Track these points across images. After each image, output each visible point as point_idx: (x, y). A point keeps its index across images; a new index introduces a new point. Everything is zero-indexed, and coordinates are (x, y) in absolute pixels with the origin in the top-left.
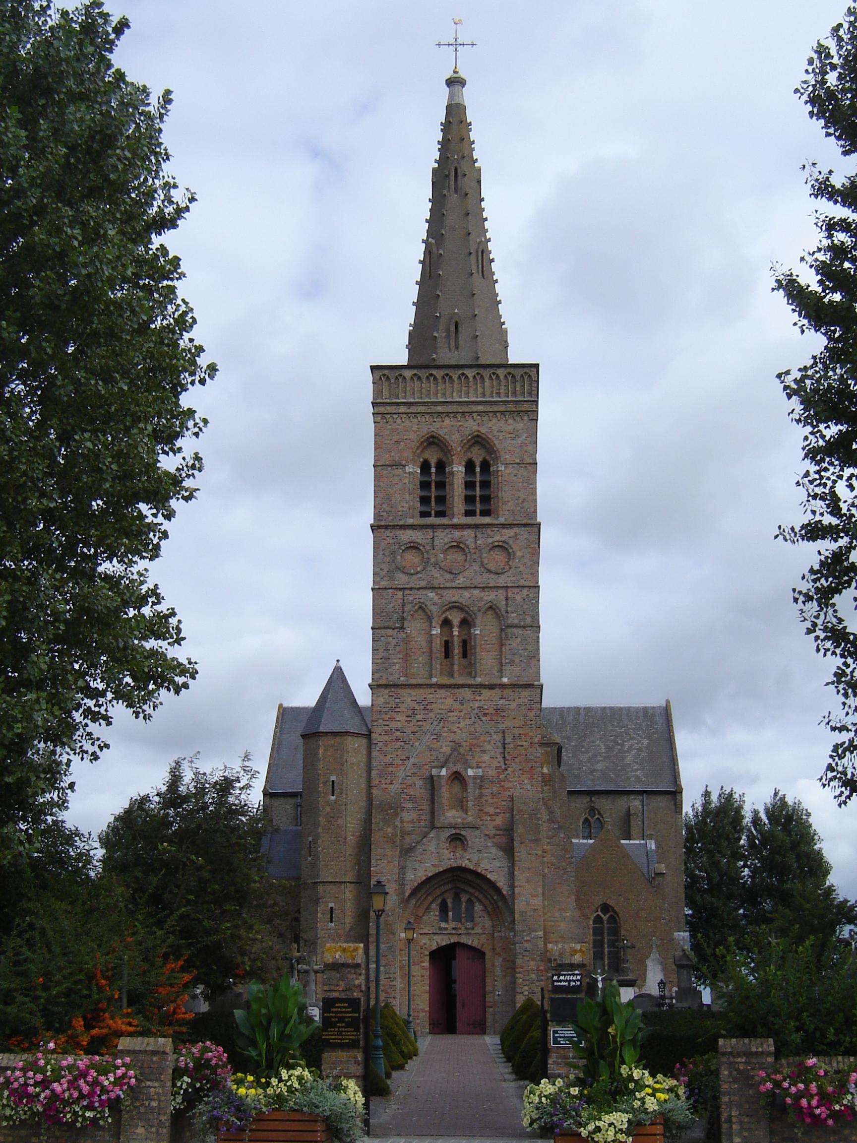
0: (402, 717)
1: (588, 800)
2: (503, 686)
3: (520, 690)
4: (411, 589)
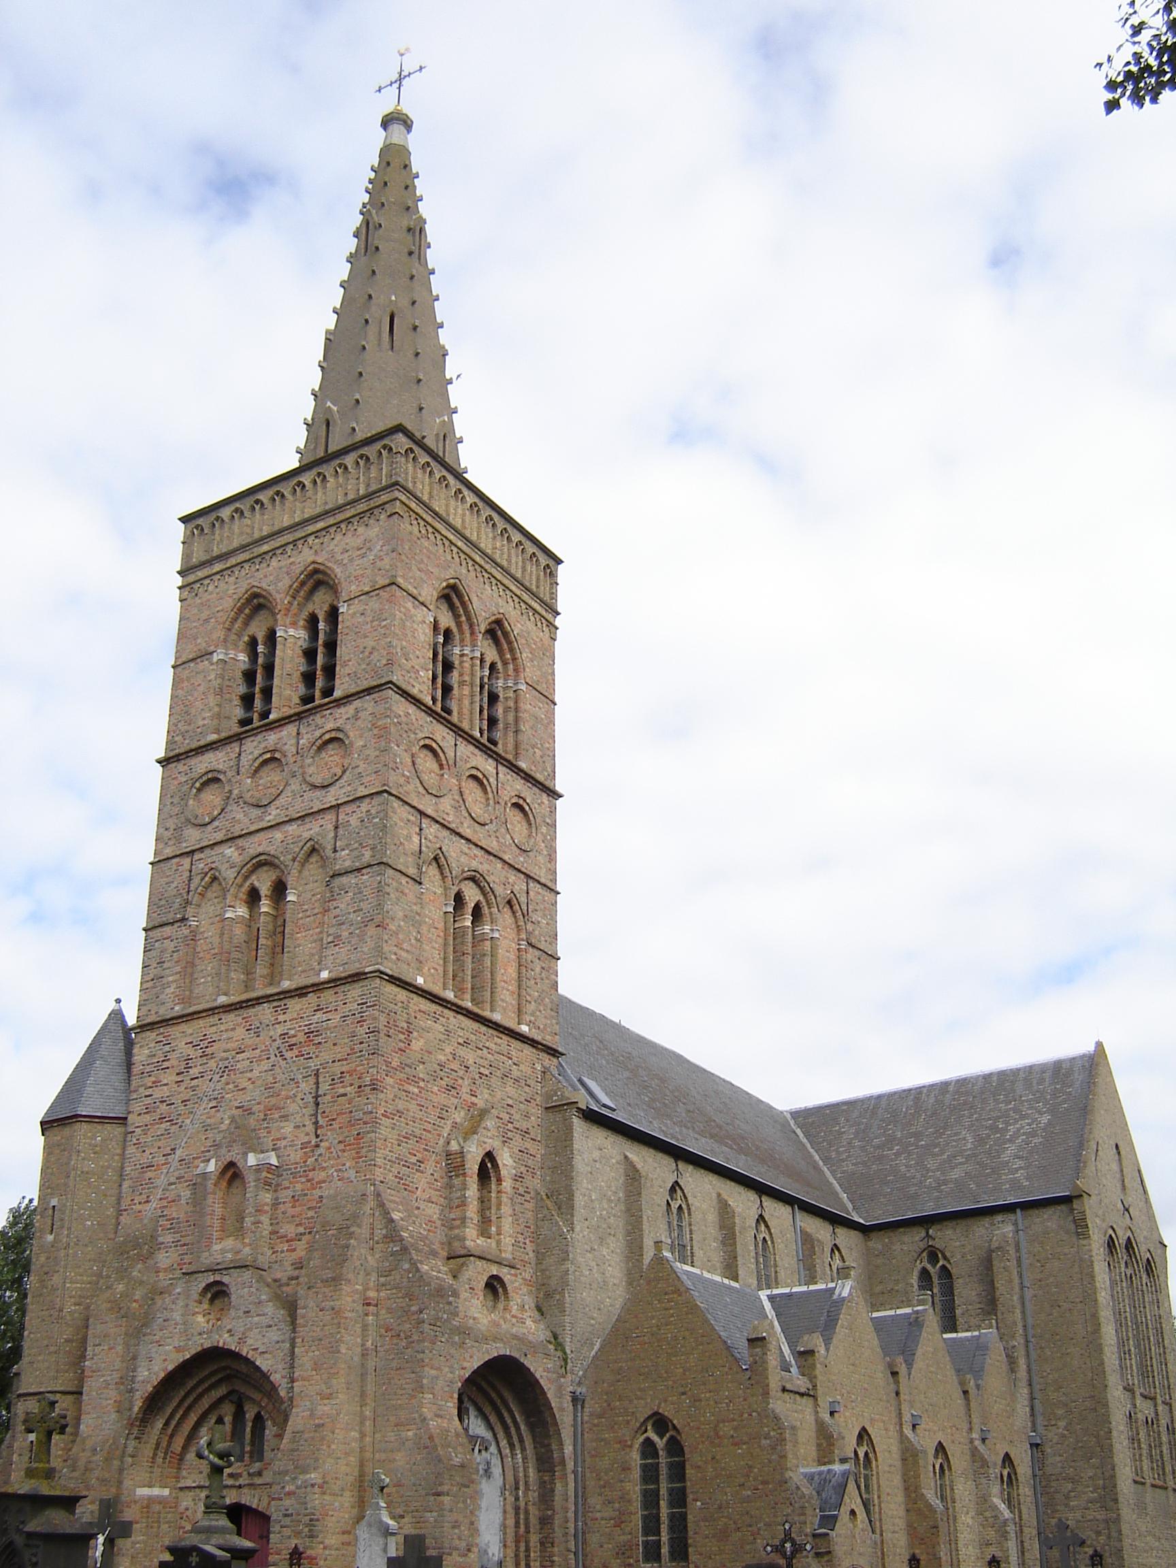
0: (169, 1078)
1: (923, 1234)
2: (318, 987)
3: (347, 987)
4: (201, 849)
